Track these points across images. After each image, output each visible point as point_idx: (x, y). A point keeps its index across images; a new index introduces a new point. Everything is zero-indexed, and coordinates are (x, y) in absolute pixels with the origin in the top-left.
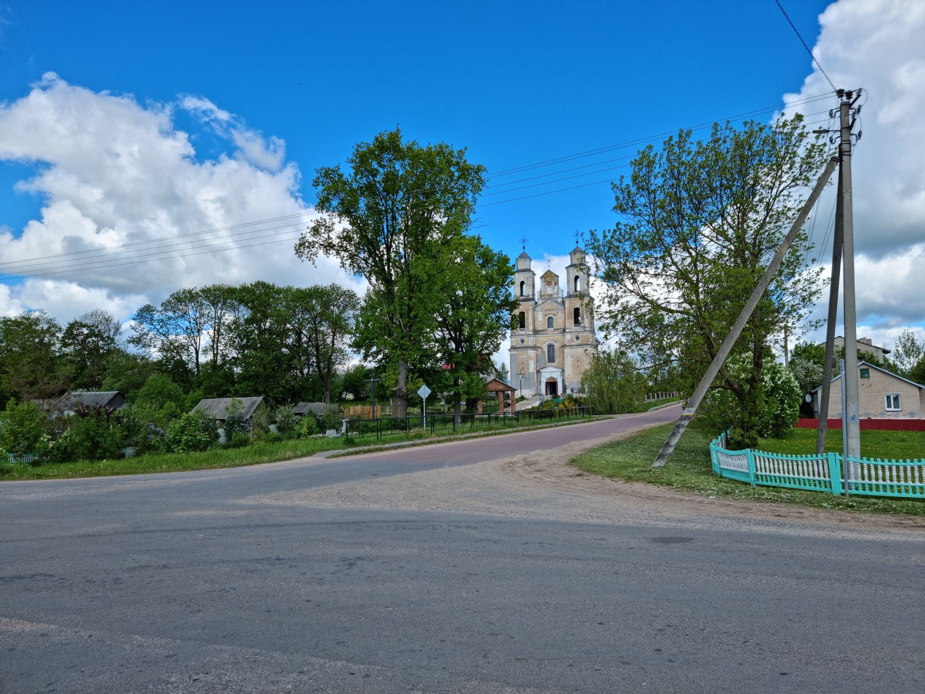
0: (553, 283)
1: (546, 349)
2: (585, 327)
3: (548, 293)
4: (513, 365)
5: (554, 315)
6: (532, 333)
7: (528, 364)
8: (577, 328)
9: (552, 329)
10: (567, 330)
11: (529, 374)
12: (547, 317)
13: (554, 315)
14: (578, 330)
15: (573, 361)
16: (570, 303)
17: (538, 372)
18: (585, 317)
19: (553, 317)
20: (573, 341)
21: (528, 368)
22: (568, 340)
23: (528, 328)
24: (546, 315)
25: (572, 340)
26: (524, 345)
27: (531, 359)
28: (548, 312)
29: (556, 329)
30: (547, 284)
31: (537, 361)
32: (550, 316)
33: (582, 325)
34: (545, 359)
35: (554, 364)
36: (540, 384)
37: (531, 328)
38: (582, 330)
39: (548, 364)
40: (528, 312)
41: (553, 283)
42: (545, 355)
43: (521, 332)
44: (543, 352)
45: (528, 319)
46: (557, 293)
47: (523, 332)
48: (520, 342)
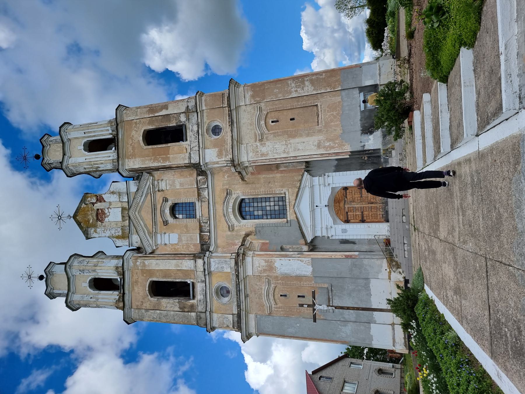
0: (98, 205)
1: (249, 224)
2: (188, 112)
3: (120, 218)
4: (291, 330)
5: (166, 200)
6: (200, 262)
7: (287, 278)
8: (189, 134)
9: (198, 205)
10: (195, 159)
11: (315, 276)
12: (170, 220)
13: (166, 200)
14: (195, 128)
15: (276, 135)
16: (133, 156)
17: (313, 246)
18: (164, 112)
19: (169, 204)
20: (224, 141)
21: (299, 278)
22: (220, 154)
23: (186, 273)
24: (166, 223)
25: (219, 146)
26: (231, 286)
27: (271, 268)
28: (159, 219)
29: (199, 195)
30: (102, 221)
31: (282, 249)
32: (167, 211)
33: (183, 118)
34: (276, 226)
35: (290, 197)
36: (353, 242)
37: (187, 264)
38: (194, 118)
39: (290, 216)
40: (151, 272)
41: (98, 205)
42: (262, 226)
43: (199, 296)
44: (258, 232)
45: (166, 273)
46: (120, 194)
47: (199, 287)
48: (226, 300)
